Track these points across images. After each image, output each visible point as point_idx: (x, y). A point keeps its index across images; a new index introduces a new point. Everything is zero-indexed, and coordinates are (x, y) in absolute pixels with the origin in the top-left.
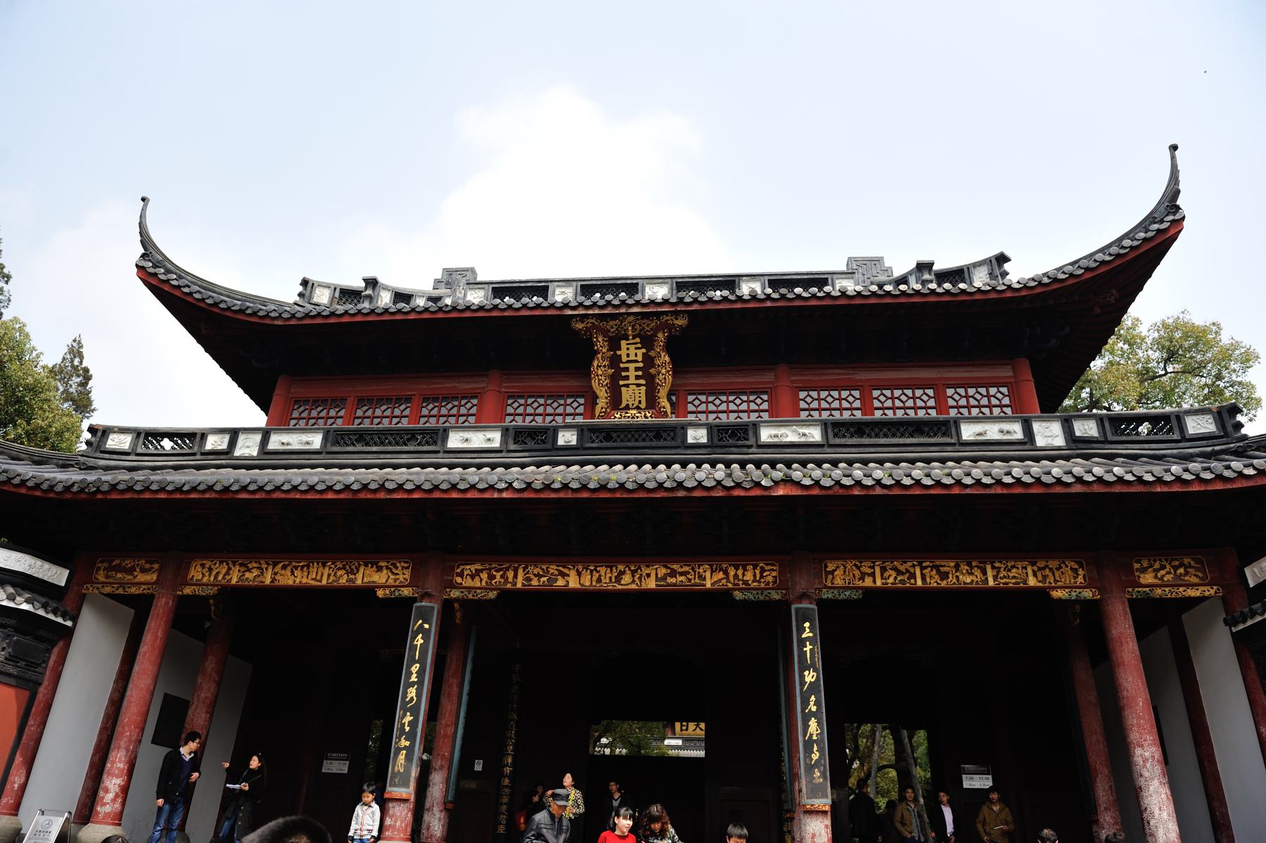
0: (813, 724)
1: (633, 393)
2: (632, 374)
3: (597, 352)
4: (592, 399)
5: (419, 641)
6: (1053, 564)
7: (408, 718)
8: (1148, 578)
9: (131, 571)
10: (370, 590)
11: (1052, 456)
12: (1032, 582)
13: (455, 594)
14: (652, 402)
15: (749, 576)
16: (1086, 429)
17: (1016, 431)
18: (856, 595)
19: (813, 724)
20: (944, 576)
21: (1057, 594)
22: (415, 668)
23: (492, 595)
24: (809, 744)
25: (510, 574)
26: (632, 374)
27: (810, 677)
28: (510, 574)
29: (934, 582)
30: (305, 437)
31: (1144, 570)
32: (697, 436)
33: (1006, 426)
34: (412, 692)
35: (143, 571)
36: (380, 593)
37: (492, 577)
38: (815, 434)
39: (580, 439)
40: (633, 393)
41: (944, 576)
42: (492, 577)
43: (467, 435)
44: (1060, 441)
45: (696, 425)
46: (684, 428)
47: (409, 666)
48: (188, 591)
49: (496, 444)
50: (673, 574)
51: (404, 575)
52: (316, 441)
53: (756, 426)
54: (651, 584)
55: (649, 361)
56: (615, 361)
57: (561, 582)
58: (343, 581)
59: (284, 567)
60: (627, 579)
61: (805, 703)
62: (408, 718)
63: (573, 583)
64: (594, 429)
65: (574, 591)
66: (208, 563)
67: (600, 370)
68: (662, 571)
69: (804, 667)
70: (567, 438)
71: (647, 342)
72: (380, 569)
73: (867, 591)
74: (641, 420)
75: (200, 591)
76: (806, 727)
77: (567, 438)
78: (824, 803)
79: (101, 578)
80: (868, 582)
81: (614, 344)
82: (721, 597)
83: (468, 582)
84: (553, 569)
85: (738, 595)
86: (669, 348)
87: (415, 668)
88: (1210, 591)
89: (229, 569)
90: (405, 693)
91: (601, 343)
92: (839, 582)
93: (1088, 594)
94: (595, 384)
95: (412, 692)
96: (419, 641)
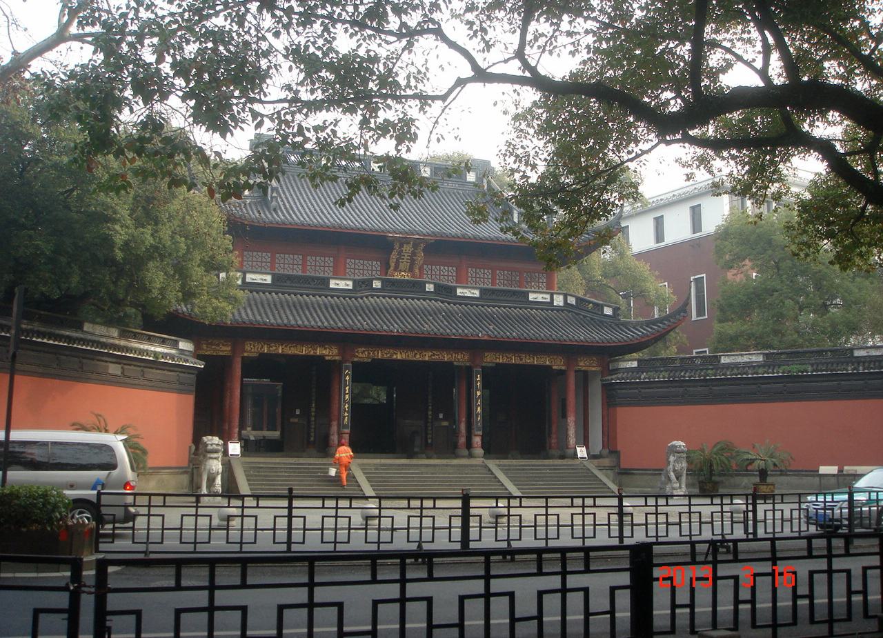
0: (479, 408)
1: (404, 264)
2: (406, 257)
3: (393, 249)
4: (388, 267)
5: (347, 378)
6: (555, 357)
7: (347, 406)
8: (581, 364)
9: (218, 345)
10: (322, 358)
11: (559, 309)
12: (548, 363)
13: (356, 359)
14: (411, 269)
15: (459, 357)
16: (572, 301)
17: (547, 298)
18: (494, 365)
19: (479, 408)
20: (521, 360)
21: (554, 367)
22: (347, 388)
23: (370, 360)
24: (477, 415)
25: (376, 353)
26: (406, 257)
27: (479, 393)
28: (376, 353)
29: (518, 362)
30: (264, 277)
31: (581, 361)
32: (430, 288)
33: (545, 296)
34: (347, 397)
35: (223, 345)
36: (327, 358)
37: (369, 353)
38: (477, 293)
39: (382, 285)
40: (404, 264)
41: (521, 360)
42: (369, 353)
43: (337, 282)
44: (561, 304)
45: (429, 283)
46: (425, 283)
47: (345, 388)
48: (246, 354)
49: (351, 288)
50: (434, 355)
51: (335, 351)
52: (268, 279)
53: (455, 289)
54: (427, 359)
55: (414, 254)
56: (400, 253)
57: (395, 357)
58: (312, 353)
59: (286, 346)
60: (418, 356)
61: (477, 402)
62: (347, 406)
63: (399, 357)
64: (389, 281)
65: (399, 360)
66: (253, 343)
67: (394, 255)
68: (430, 354)
69: (477, 390)
70: (377, 284)
71: (416, 246)
72: (325, 349)
73: (497, 364)
74: (406, 278)
75: (251, 355)
76: (477, 409)
77: (377, 284)
78: (480, 433)
79: (205, 347)
80: (498, 360)
81: (401, 245)
82: (451, 363)
83: (361, 355)
84: (391, 351)
85: (455, 363)
86: (424, 250)
87: (347, 388)
88: (598, 369)
89: (262, 346)
90: (344, 398)
91: (397, 246)
92: (488, 360)
93: (563, 368)
94: (391, 261)
95: (347, 397)
96: (347, 378)
